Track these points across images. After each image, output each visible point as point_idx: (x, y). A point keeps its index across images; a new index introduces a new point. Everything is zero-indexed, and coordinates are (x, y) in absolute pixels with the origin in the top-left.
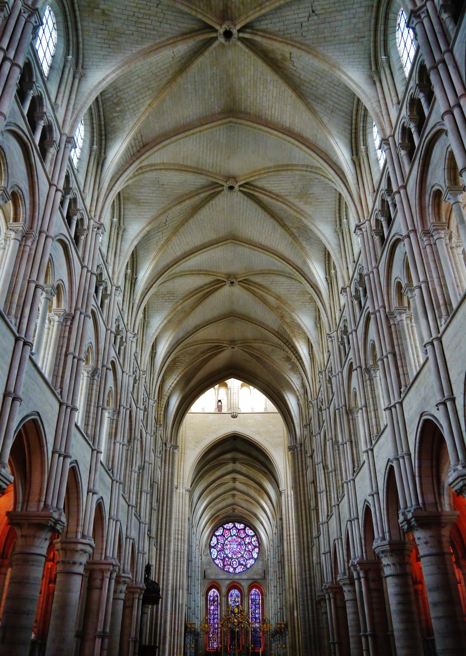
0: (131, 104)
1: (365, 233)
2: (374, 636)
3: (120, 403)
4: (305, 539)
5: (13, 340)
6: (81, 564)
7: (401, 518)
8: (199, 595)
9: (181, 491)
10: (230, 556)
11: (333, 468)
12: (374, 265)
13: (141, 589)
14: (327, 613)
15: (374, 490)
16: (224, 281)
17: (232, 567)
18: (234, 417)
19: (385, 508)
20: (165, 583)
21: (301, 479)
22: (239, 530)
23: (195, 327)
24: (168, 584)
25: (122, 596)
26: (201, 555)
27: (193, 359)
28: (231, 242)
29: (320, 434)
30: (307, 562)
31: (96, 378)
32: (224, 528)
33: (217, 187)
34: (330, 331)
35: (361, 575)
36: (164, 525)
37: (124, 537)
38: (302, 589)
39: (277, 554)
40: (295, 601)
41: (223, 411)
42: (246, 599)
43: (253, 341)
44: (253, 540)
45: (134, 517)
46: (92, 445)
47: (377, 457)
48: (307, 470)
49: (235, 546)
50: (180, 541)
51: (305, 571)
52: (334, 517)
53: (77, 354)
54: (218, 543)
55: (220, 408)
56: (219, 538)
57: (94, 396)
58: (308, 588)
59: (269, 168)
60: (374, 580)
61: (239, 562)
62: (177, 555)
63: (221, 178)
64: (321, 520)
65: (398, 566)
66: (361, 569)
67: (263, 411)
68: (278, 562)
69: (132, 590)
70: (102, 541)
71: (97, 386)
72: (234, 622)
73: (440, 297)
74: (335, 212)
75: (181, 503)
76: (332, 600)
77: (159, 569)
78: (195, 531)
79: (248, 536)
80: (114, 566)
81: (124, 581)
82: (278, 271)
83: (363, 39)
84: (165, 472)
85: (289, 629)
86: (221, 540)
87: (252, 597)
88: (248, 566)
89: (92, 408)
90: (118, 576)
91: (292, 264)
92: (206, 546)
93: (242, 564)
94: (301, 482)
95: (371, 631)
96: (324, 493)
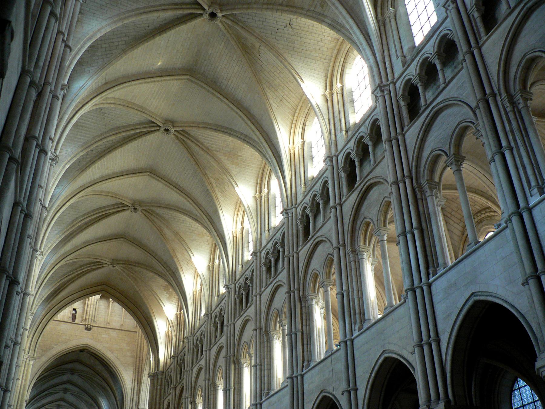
0: (105, 43)
1: (290, 218)
12: (295, 250)
16: (127, 206)
18: (88, 330)
23: (84, 243)
27: (71, 271)
28: (148, 175)
33: (154, 126)
34: (229, 283)
41: (77, 321)
43: (137, 265)
55: (74, 317)
59: (209, 124)
63: (160, 120)
73: (357, 307)
74: (258, 178)
82: (185, 210)
83: (324, 61)
91: (203, 209)
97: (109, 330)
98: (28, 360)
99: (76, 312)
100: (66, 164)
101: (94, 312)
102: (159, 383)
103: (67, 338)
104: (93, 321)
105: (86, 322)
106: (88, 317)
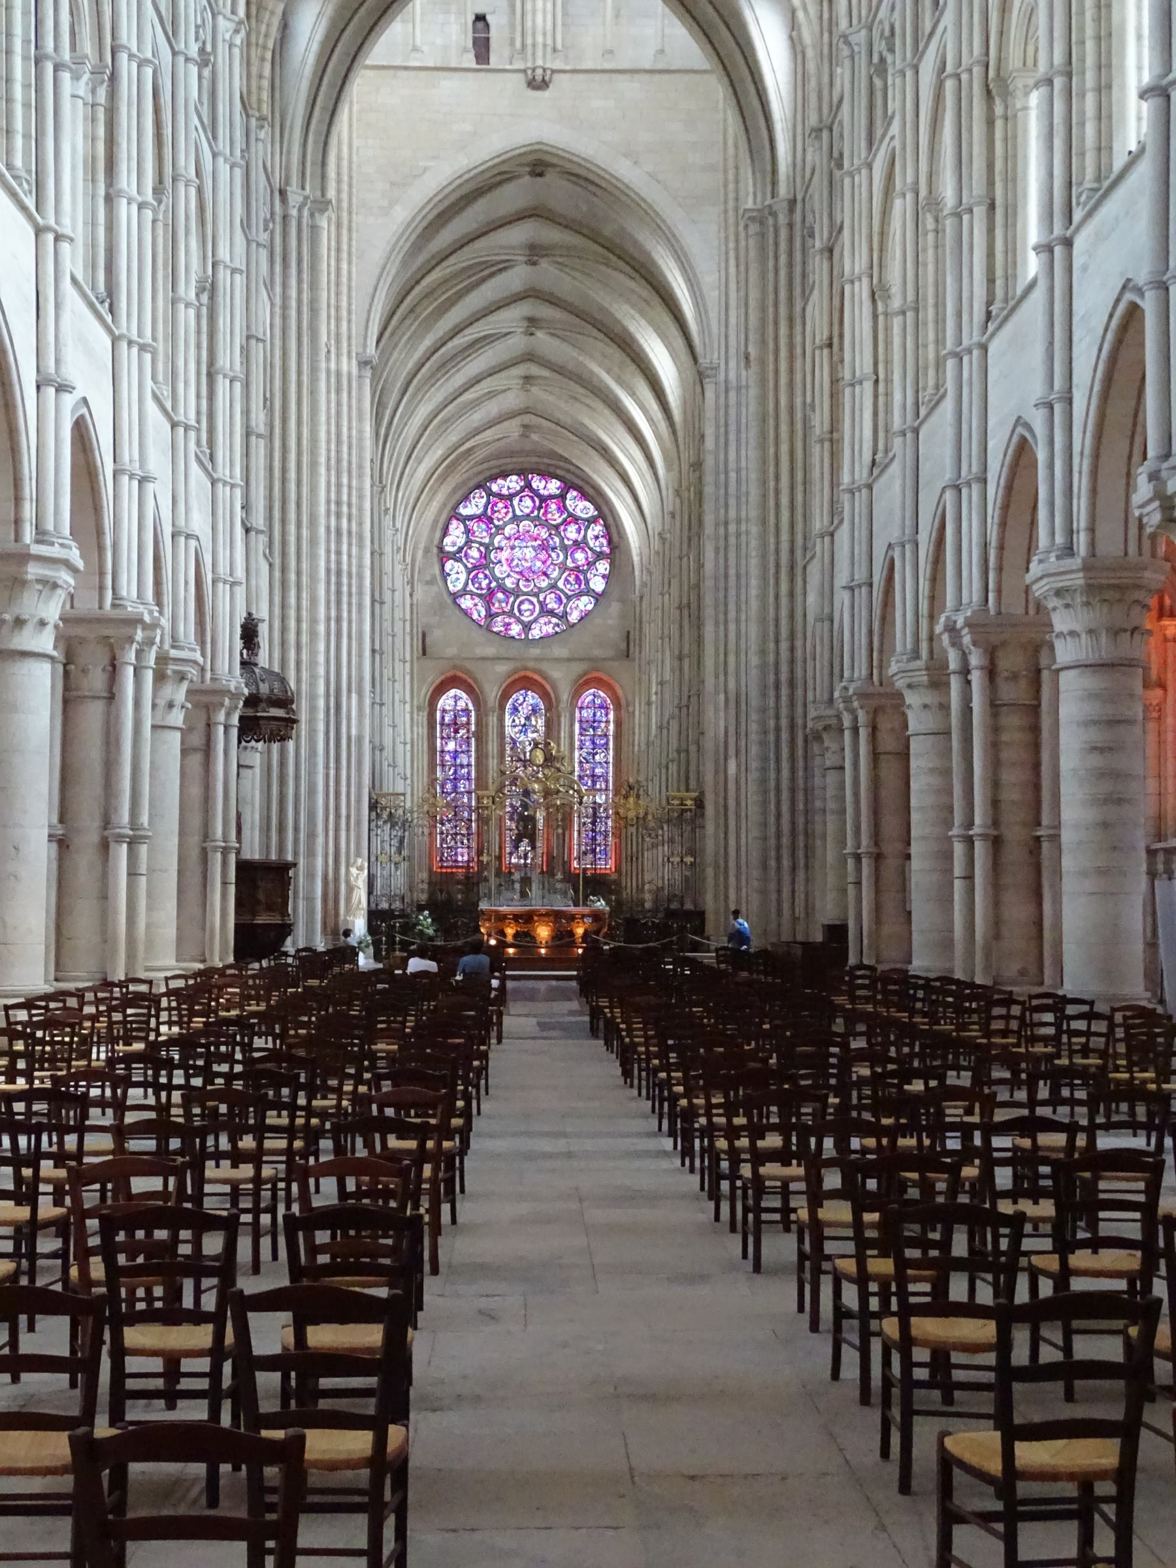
2: (996, 843)
4: (785, 537)
6: (42, 623)
7: (1143, 490)
8: (408, 707)
9: (345, 367)
10: (509, 583)
11: (910, 297)
13: (234, 696)
14: (842, 768)
15: (1057, 385)
17: (519, 621)
19: (1087, 451)
20: (305, 675)
21: (783, 331)
22: (544, 499)
24: (313, 677)
25: (177, 718)
26: (411, 582)
29: (870, 167)
30: (784, 613)
32: (490, 493)
35: (975, 660)
36: (292, 487)
37: (168, 530)
38: (764, 695)
39: (675, 583)
40: (732, 730)
41: (494, 61)
42: (564, 722)
44: (590, 534)
45: (195, 468)
46: (33, 209)
47: (1085, 268)
48: (806, 298)
49: (530, 553)
50: (345, 539)
51: (777, 642)
52: (895, 468)
54: (468, 543)
55: (482, 49)
56: (474, 525)
58: (784, 691)
60: (1014, 677)
61: (542, 604)
62: (339, 584)
64: (846, 479)
65: (1104, 639)
66: (975, 643)
67: (647, 66)
68: (680, 608)
69: (205, 699)
70: (101, 548)
75: (345, 408)
76: (863, 733)
77: (284, 630)
78: (390, 504)
79: (576, 519)
80: (146, 626)
81: (175, 672)
84: (285, 297)
85: (710, 810)
86: (479, 529)
87: (585, 713)
88: (574, 617)
90: (162, 659)
92: (427, 551)
93: (551, 613)
94: (783, 342)
95: (984, 826)
96: (868, 386)
97: (614, 76)
98: (306, 213)
99: (487, 26)
101: (549, 17)
102: (783, 246)
103: (468, 127)
104: (549, 50)
105: (525, 59)
106: (529, 41)
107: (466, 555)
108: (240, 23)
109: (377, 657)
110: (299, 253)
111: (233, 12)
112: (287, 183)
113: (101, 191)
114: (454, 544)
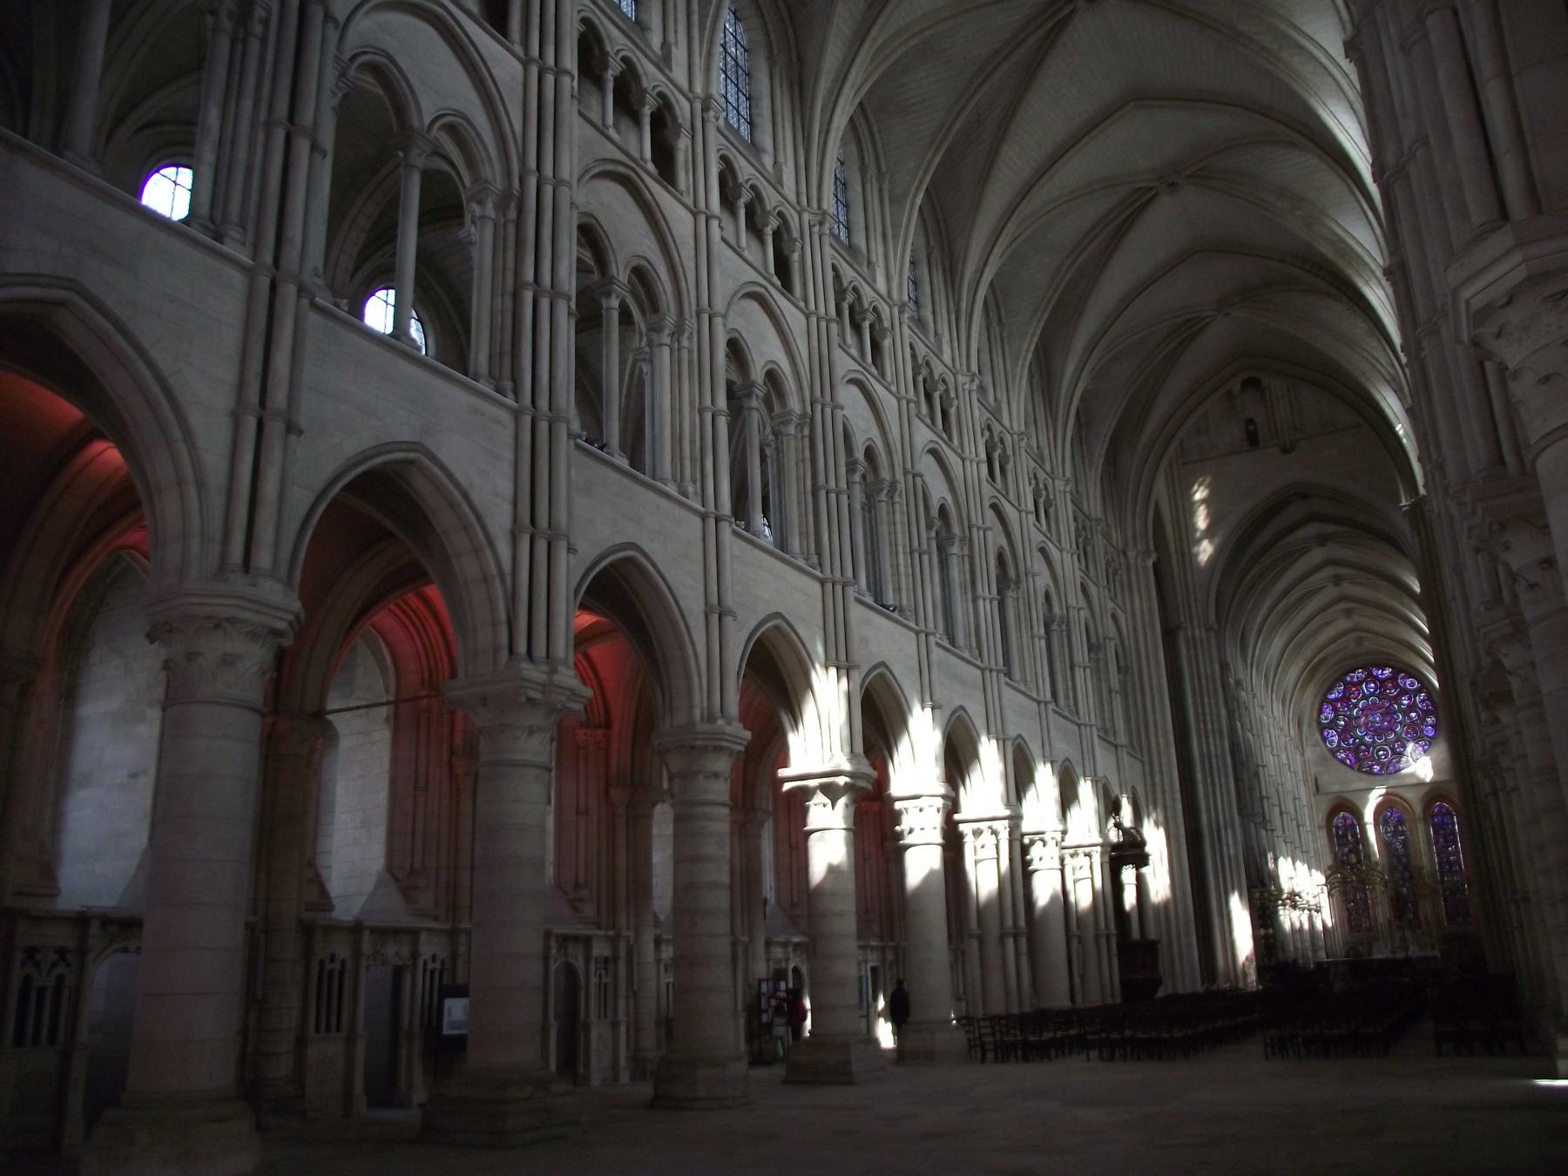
3: (969, 521)
5: (697, 521)
9: (1197, 633)
22: (1383, 682)
31: (897, 499)
32: (1346, 683)
53: (832, 484)
55: (1253, 439)
57: (900, 536)
62: (1210, 763)
71: (902, 513)
72: (1352, 880)
79: (1404, 692)
84: (1133, 609)
89: (901, 556)
92: (1310, 725)
98: (1139, 560)
100: (915, 196)
107: (1337, 725)
108: (1068, 480)
109: (1265, 801)
110: (1138, 581)
111: (1064, 476)
112: (1127, 545)
113: (970, 596)
114: (1326, 719)
